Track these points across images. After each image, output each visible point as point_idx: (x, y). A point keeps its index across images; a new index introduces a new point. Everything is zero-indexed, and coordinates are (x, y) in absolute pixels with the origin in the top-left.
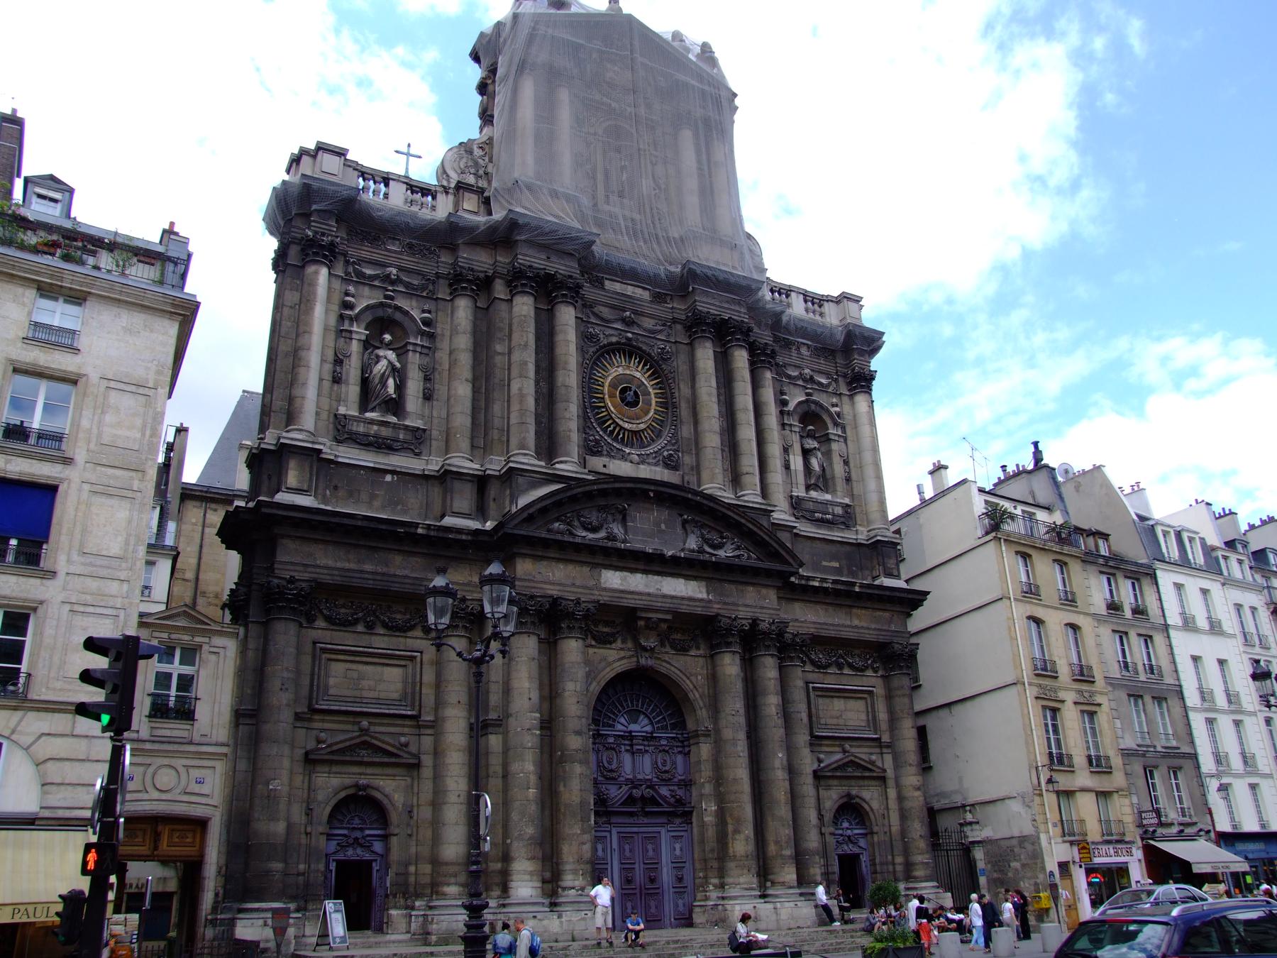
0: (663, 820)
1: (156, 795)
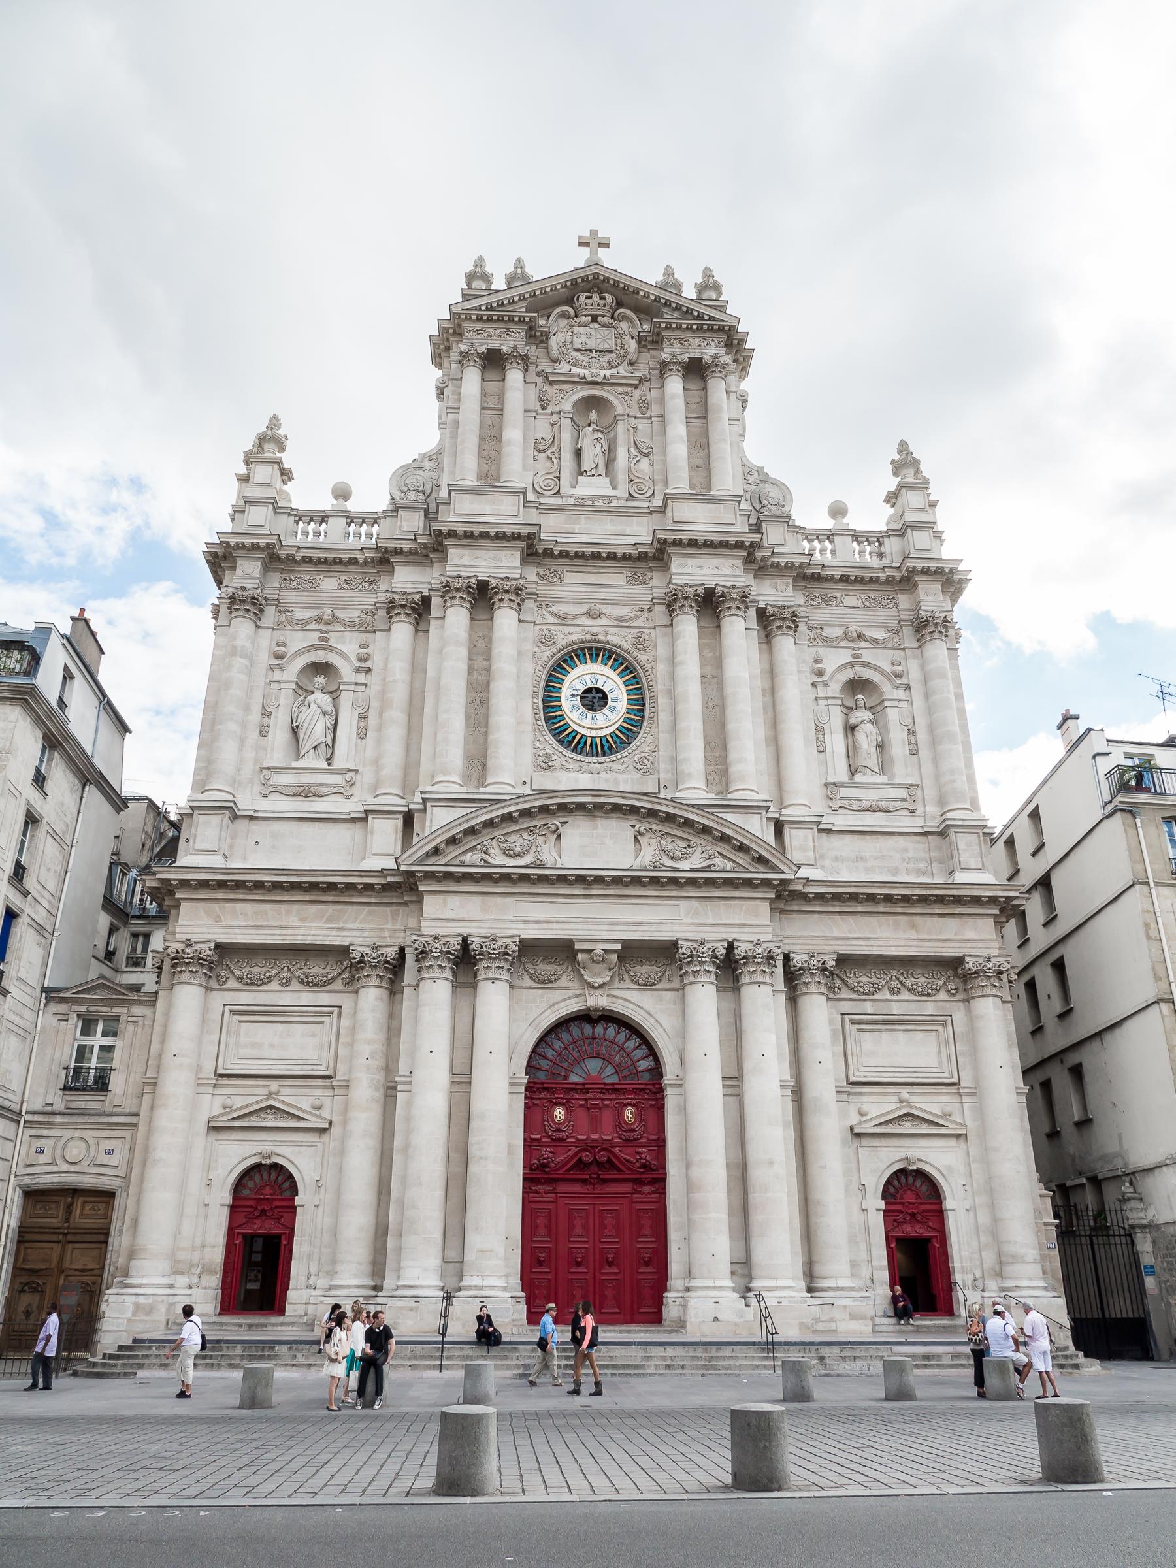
0: (626, 1187)
1: (65, 1167)
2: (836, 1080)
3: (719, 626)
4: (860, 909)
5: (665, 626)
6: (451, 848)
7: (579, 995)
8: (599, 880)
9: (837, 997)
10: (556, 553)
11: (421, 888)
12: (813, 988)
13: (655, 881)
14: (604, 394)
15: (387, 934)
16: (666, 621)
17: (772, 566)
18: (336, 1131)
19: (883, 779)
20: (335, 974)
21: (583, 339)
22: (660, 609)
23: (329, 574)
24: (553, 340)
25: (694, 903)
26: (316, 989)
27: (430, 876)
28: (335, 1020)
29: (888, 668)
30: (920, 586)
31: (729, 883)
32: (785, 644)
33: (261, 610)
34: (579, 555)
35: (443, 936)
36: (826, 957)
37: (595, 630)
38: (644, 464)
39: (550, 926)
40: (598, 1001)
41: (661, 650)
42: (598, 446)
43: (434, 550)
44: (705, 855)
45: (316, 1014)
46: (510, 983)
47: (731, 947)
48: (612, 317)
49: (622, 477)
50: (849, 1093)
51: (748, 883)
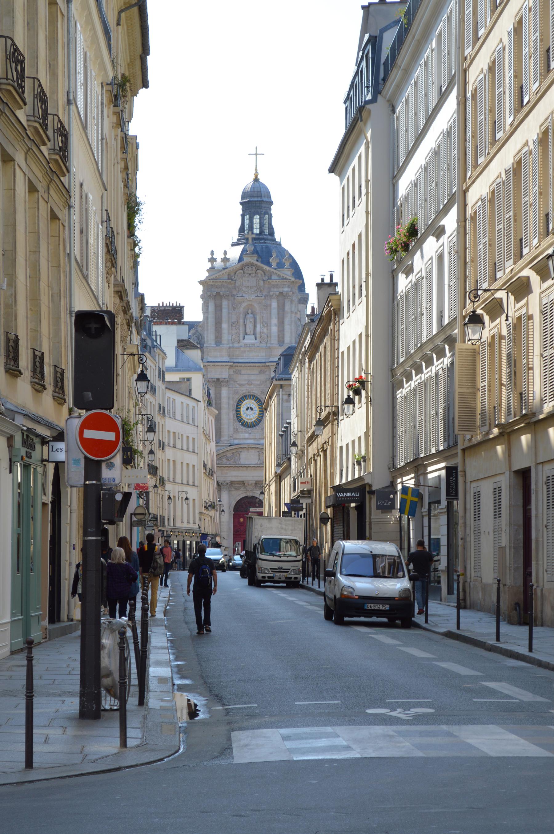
40: (250, 494)
49: (258, 336)
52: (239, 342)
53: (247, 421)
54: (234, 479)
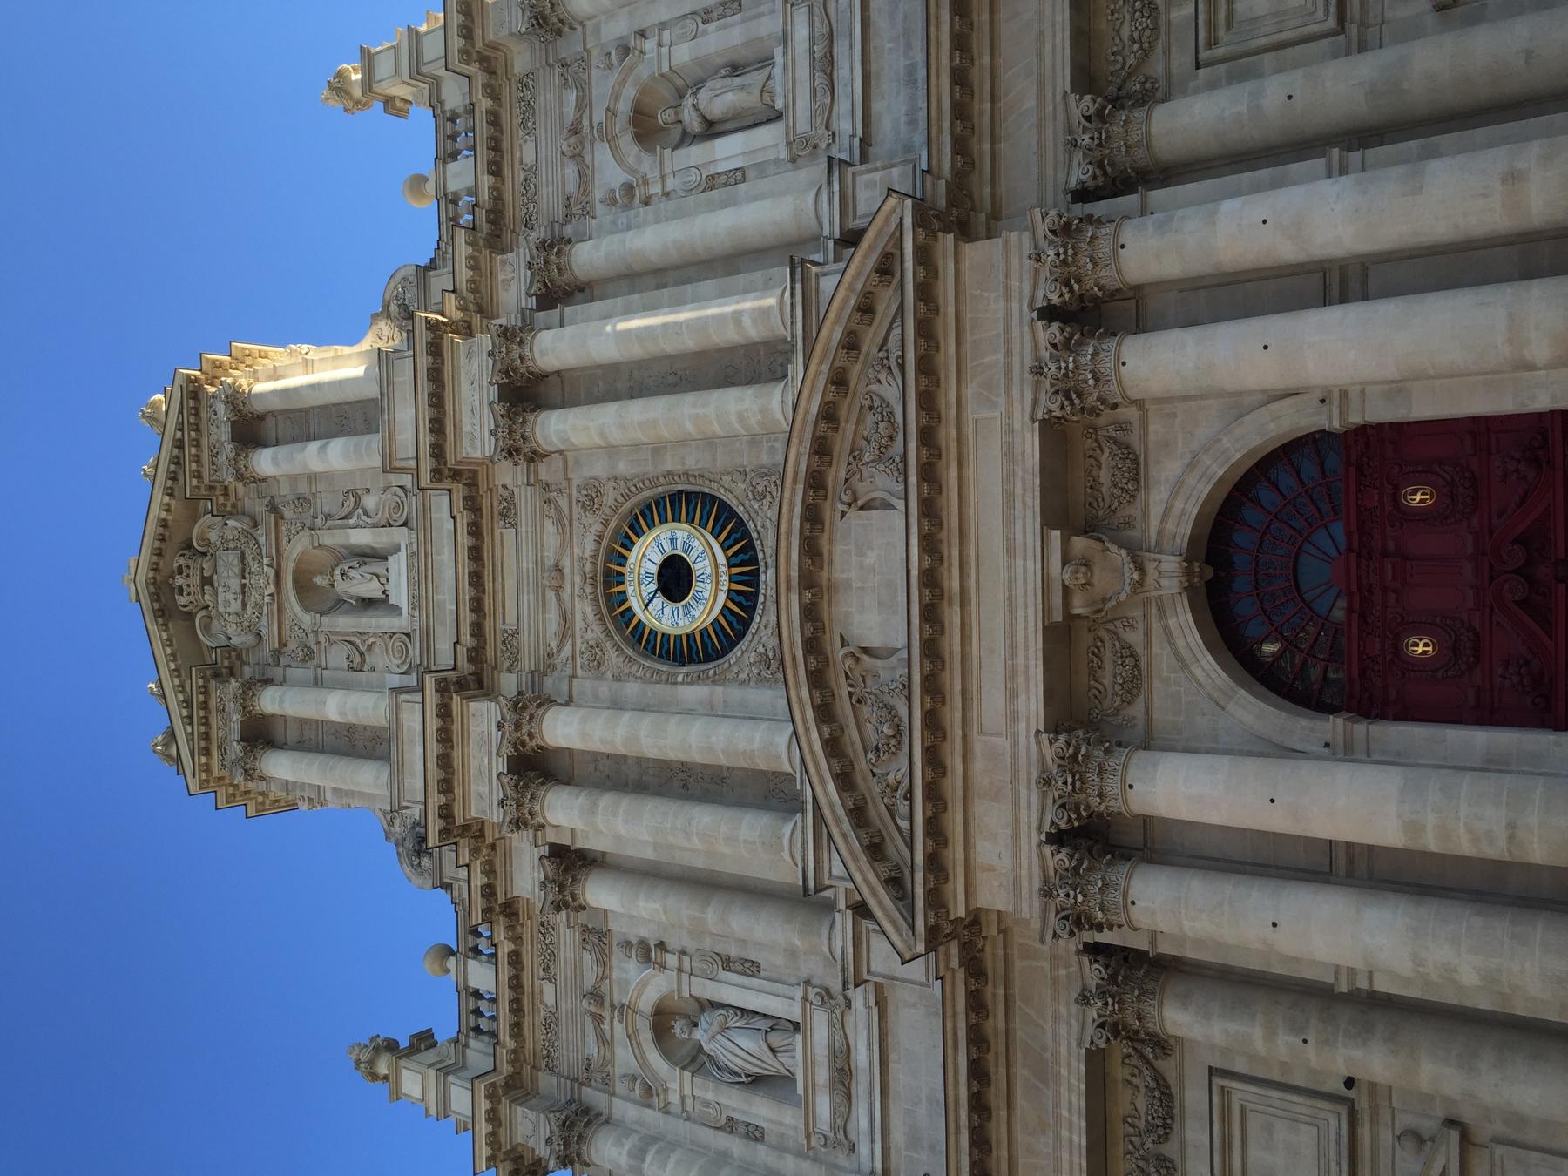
2: (1335, 56)
3: (558, 373)
4: (986, 60)
5: (565, 462)
6: (890, 850)
7: (1160, 607)
8: (931, 580)
9: (1162, 82)
10: (474, 643)
11: (961, 913)
12: (1136, 134)
13: (929, 473)
14: (291, 565)
15: (1063, 972)
16: (557, 461)
17: (473, 291)
18: (1467, 1114)
19: (778, 52)
20: (1146, 1072)
21: (230, 597)
22: (544, 471)
23: (537, 996)
24: (235, 641)
25: (970, 392)
26: (1177, 1111)
27: (936, 900)
28: (1234, 1084)
29: (615, 76)
30: (491, 37)
31: (925, 330)
32: (587, 257)
33: (587, 1111)
34: (477, 607)
35: (1046, 880)
36: (1077, 116)
37: (578, 579)
38: (370, 502)
39: (1021, 668)
40: (1168, 575)
41: (599, 469)
42: (353, 573)
43: (481, 835)
44: (882, 377)
45: (1226, 1119)
46: (1138, 748)
47: (1049, 313)
48: (205, 554)
50: (1363, 25)
51: (925, 292)
52: (408, 635)
53: (722, 597)
54: (1033, 705)
